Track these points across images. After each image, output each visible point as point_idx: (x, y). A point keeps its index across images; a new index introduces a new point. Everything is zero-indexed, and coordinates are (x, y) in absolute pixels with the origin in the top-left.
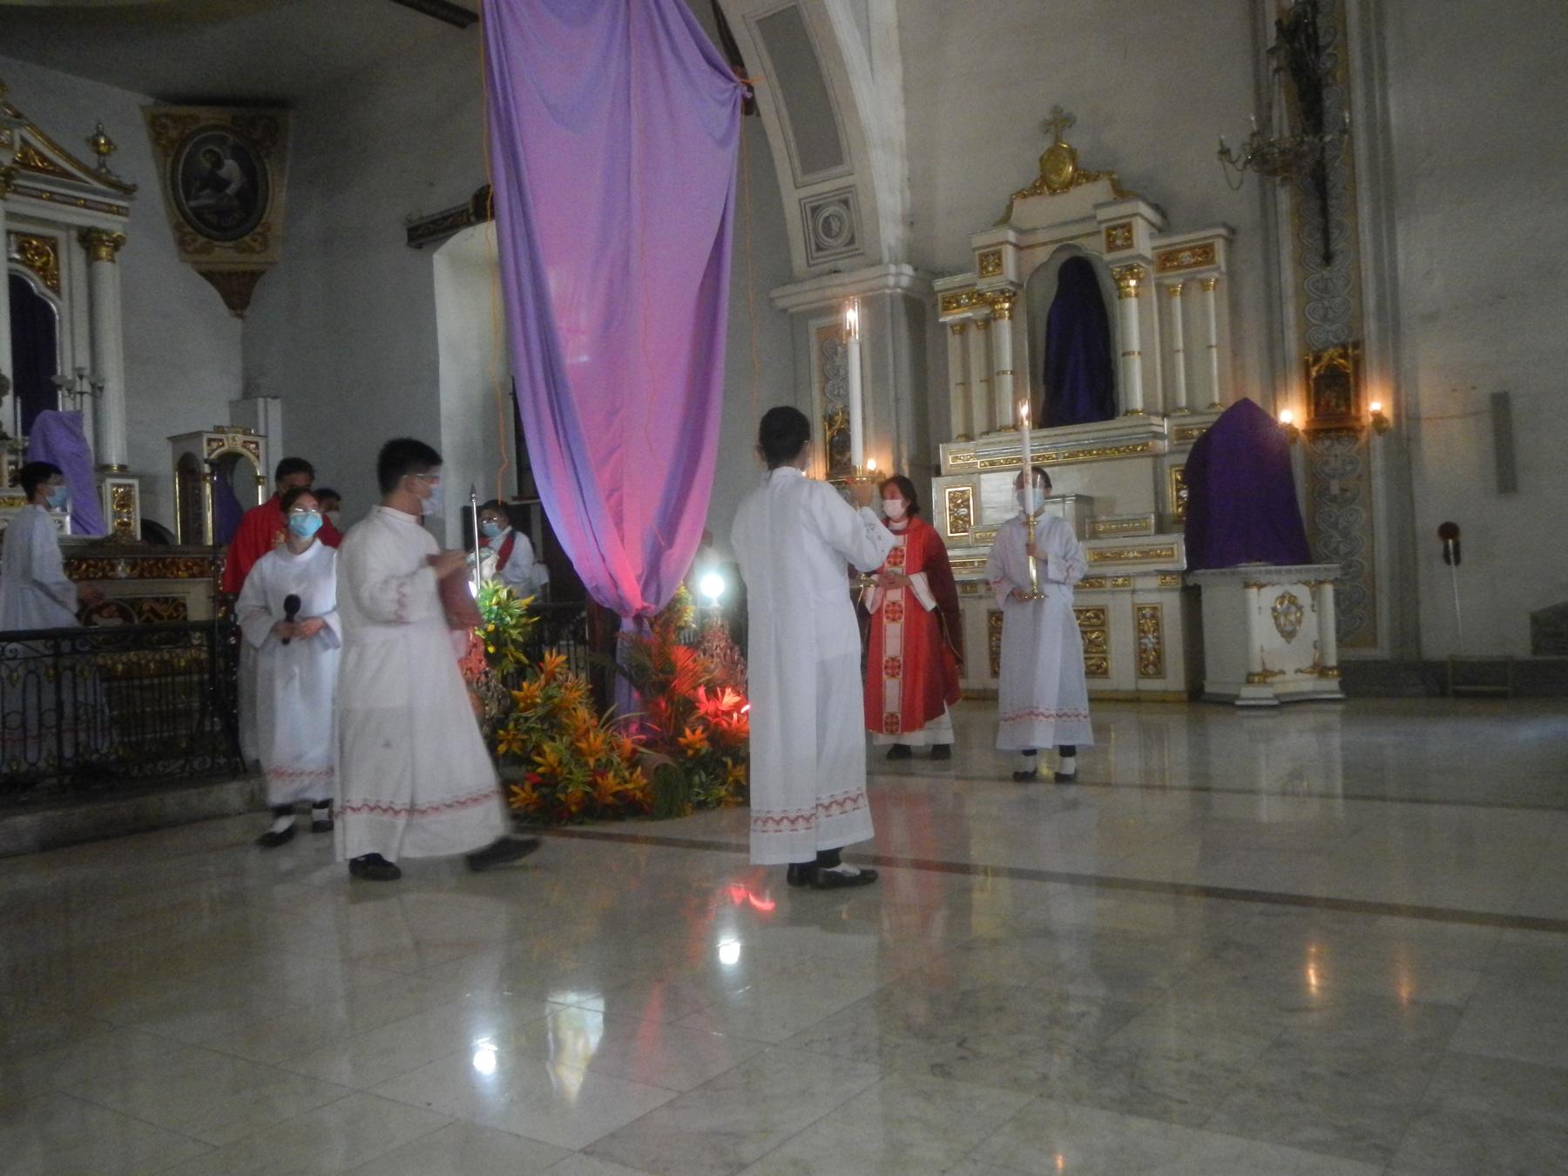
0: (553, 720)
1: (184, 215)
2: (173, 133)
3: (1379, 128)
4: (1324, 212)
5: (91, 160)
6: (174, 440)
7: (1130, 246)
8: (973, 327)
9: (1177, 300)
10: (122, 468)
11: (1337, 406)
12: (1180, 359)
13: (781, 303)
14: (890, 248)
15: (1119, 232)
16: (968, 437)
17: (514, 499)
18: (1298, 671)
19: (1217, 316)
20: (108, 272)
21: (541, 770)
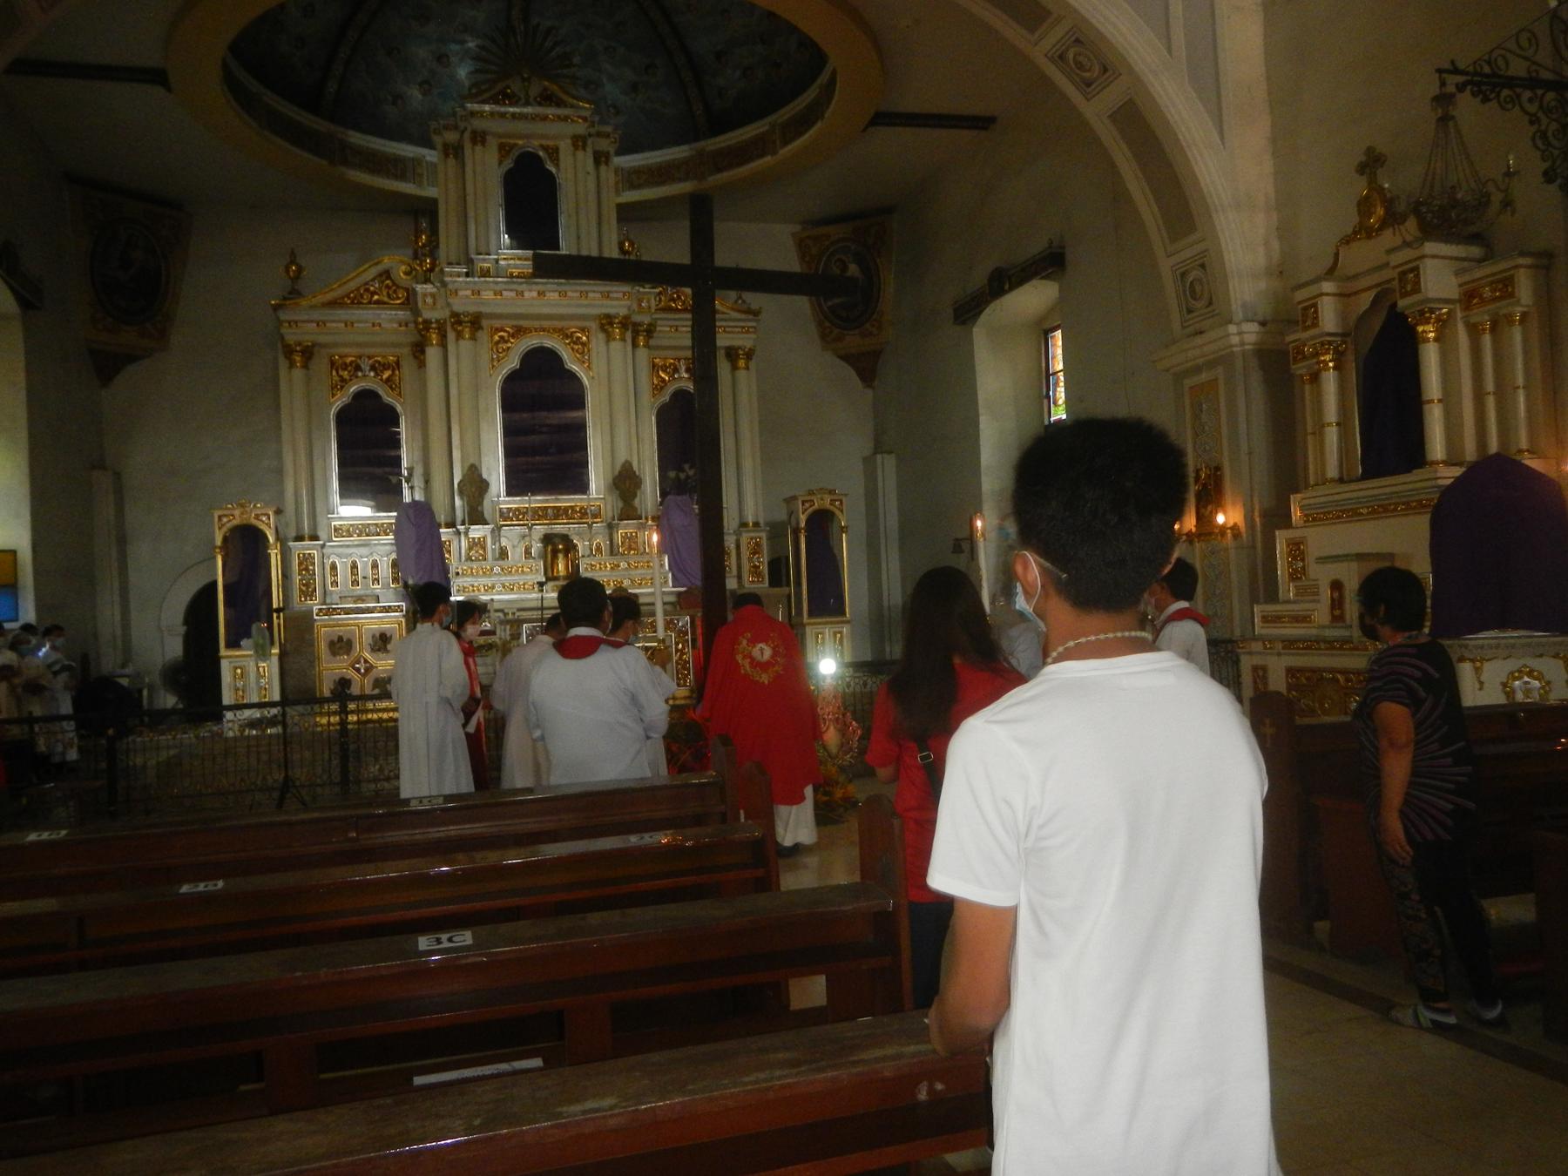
9: (1487, 339)
10: (756, 524)
12: (1491, 402)
14: (1244, 306)
19: (1526, 352)
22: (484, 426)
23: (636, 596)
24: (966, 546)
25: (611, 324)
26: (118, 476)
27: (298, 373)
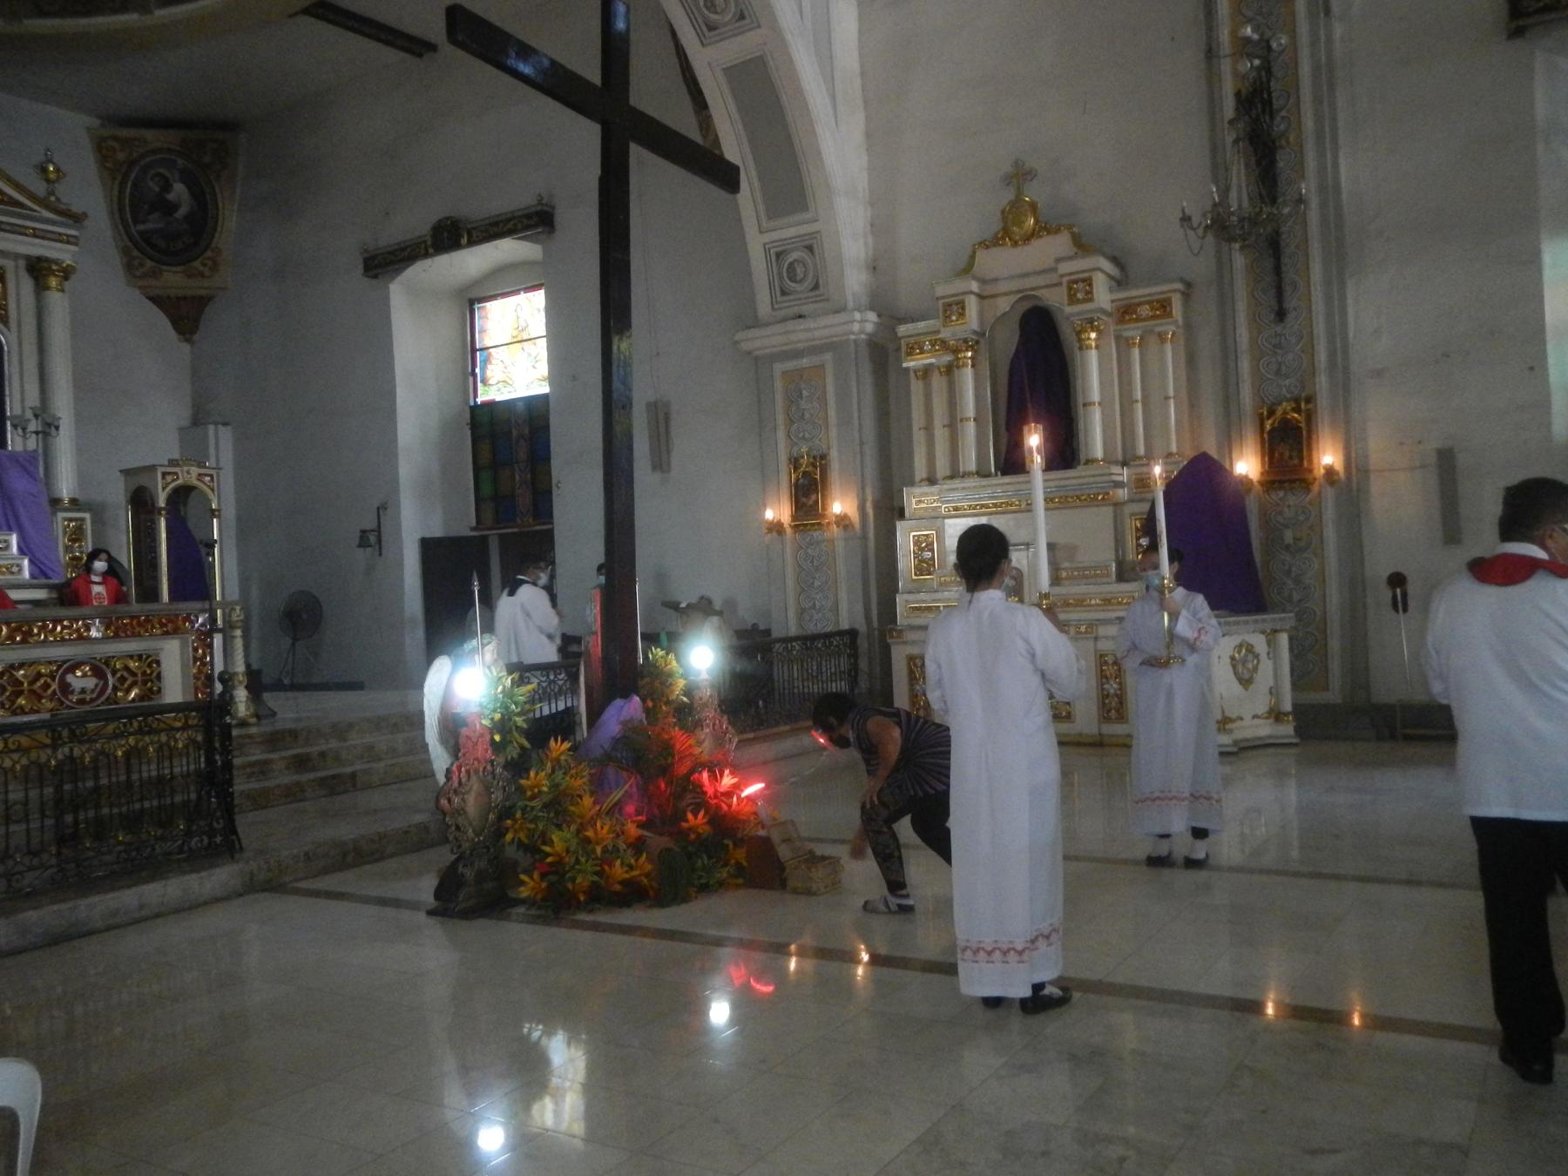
0: (558, 806)
1: (131, 238)
2: (121, 156)
3: (1330, 189)
4: (1278, 270)
5: (40, 188)
6: (127, 473)
7: (1091, 300)
8: (936, 373)
9: (1136, 352)
10: (73, 501)
11: (1291, 457)
13: (745, 346)
15: (1081, 285)
16: (931, 481)
17: (473, 529)
18: (1255, 717)
20: (57, 301)
21: (549, 860)
24: (372, 539)
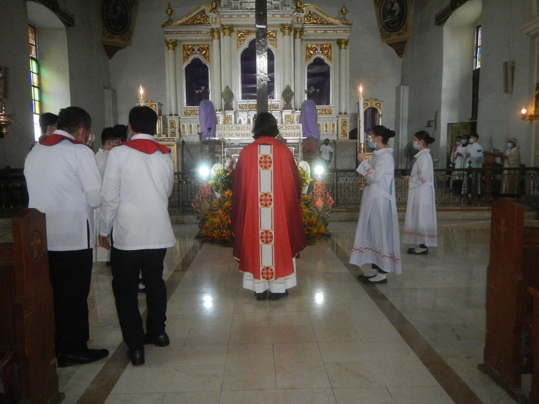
10: (346, 113)
17: (470, 120)
22: (233, 72)
23: (286, 140)
24: (433, 124)
25: (284, 28)
26: (114, 91)
27: (171, 52)
